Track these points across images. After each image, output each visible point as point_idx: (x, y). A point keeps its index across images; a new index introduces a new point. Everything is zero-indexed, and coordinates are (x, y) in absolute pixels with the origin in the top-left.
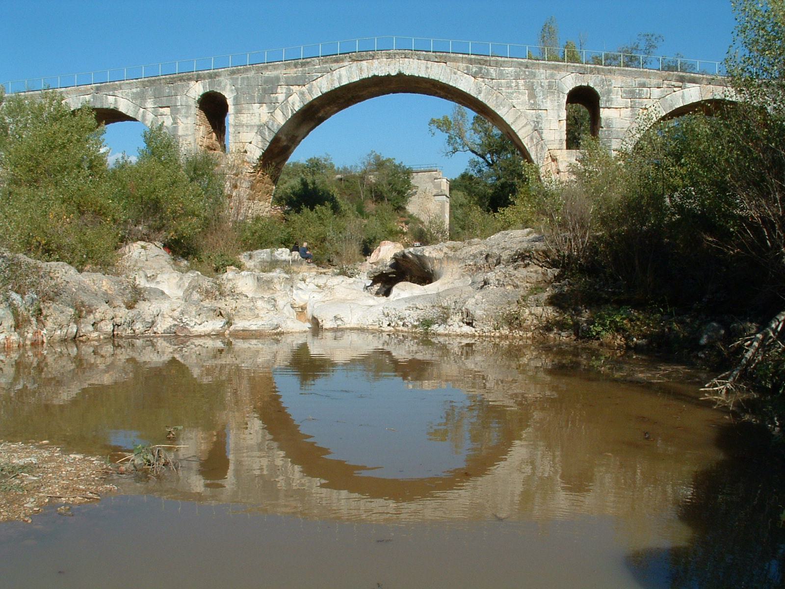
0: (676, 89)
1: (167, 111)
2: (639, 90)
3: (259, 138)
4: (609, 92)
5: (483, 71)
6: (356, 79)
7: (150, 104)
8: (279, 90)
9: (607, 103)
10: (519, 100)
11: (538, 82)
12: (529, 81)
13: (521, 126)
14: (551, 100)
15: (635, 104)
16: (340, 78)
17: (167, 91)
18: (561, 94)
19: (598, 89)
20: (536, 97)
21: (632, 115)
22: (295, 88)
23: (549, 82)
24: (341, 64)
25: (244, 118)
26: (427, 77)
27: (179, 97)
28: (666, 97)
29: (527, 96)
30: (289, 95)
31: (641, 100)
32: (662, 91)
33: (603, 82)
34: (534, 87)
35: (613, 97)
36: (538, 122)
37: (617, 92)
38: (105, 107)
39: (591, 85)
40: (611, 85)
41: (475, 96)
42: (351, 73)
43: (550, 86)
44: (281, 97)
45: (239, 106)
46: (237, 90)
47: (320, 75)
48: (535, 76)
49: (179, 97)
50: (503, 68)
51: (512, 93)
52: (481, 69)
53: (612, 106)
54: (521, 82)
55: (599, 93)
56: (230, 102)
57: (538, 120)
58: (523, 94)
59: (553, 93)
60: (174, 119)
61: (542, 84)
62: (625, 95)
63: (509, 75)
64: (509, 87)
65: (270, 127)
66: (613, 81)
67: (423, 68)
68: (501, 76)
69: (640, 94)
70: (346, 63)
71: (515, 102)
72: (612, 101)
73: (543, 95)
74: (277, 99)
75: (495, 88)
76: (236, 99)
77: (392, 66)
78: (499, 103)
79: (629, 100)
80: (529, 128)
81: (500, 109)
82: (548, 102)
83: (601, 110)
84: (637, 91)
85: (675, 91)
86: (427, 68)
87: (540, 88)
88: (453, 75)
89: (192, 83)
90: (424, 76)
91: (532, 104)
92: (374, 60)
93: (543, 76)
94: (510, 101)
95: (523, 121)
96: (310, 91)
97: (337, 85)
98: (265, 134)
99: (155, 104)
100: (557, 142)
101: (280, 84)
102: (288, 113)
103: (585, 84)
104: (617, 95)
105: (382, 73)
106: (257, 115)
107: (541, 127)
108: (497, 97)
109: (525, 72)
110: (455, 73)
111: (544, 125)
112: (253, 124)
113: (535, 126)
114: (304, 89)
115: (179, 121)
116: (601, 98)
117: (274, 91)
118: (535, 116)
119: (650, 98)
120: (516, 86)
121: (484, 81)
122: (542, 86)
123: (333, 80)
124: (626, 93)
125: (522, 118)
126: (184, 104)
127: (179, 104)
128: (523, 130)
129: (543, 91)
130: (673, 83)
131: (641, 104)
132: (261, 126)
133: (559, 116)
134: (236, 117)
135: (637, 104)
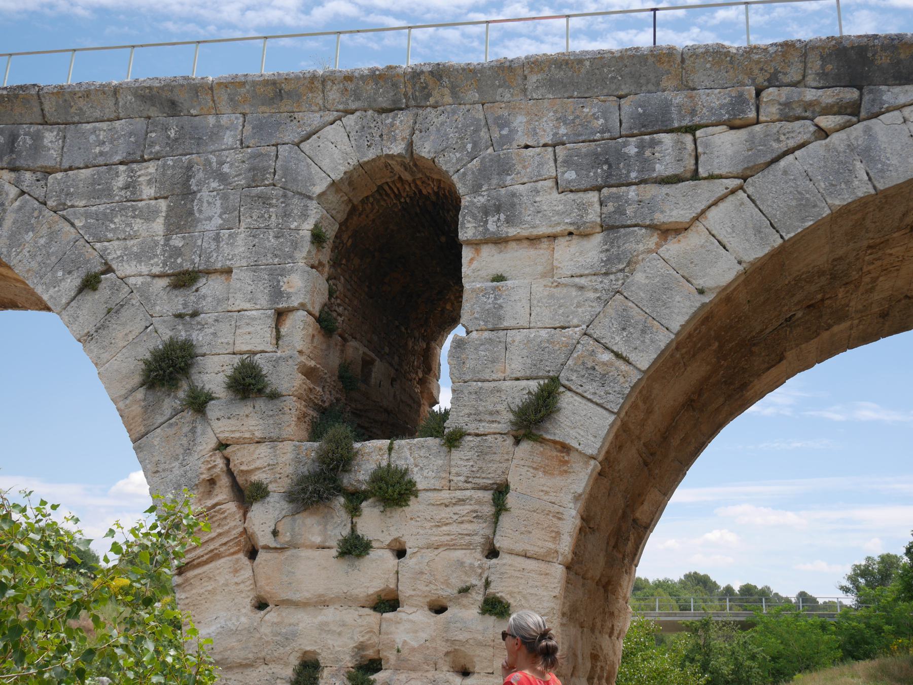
0: (826, 122)
2: (641, 147)
9: (491, 220)
10: (130, 243)
11: (208, 162)
14: (253, 232)
15: (620, 211)
21: (609, 261)
23: (254, 156)
28: (783, 163)
29: (160, 220)
32: (751, 140)
33: (476, 131)
34: (193, 181)
39: (425, 150)
40: (506, 140)
50: (89, 126)
51: (107, 218)
58: (149, 216)
59: (265, 200)
62: (571, 175)
66: (519, 121)
72: (513, 205)
73: (225, 210)
75: (51, 203)
79: (593, 197)
82: (241, 239)
83: (467, 254)
84: (632, 150)
85: (823, 133)
87: (214, 185)
94: (98, 246)
108: (53, 236)
116: (464, 202)
120: (127, 187)
121: (16, 183)
124: (578, 168)
125: (125, 313)
129: (225, 197)
130: (810, 95)
133: (277, 293)
135: (629, 211)
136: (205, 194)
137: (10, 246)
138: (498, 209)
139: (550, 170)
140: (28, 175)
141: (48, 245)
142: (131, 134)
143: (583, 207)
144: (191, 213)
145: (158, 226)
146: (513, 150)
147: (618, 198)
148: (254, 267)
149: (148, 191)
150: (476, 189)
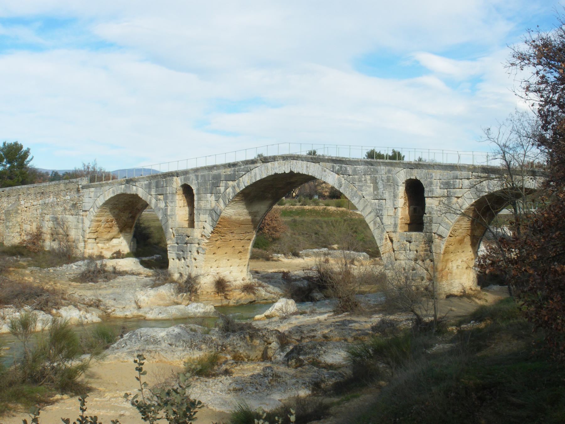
1: (161, 197)
2: (453, 181)
3: (210, 218)
4: (431, 183)
5: (343, 169)
6: (264, 176)
7: (153, 192)
8: (221, 184)
11: (379, 177)
12: (374, 176)
13: (367, 213)
14: (389, 192)
16: (255, 175)
17: (162, 183)
18: (396, 186)
19: (422, 181)
20: (378, 189)
22: (230, 183)
23: (387, 176)
24: (256, 165)
25: (203, 204)
26: (307, 174)
27: (168, 188)
30: (226, 189)
31: (455, 190)
35: (434, 188)
36: (380, 210)
37: (437, 183)
38: (132, 193)
39: (418, 178)
40: (431, 178)
41: (338, 189)
42: (262, 172)
43: (388, 179)
44: (222, 189)
45: (199, 195)
46: (198, 183)
47: (244, 173)
48: (377, 172)
49: (168, 188)
51: (362, 186)
52: (341, 167)
53: (434, 196)
54: (368, 177)
55: (423, 184)
56: (195, 192)
57: (380, 208)
58: (369, 187)
59: (390, 185)
60: (166, 203)
61: (383, 178)
62: (442, 186)
63: (360, 172)
64: (360, 181)
65: (216, 211)
66: (434, 174)
67: (305, 168)
68: (355, 172)
69: (454, 185)
70: (258, 165)
71: (364, 193)
74: (220, 190)
76: (198, 190)
77: (286, 166)
78: (353, 195)
80: (373, 214)
81: (354, 200)
82: (387, 193)
83: (426, 199)
86: (307, 167)
88: (323, 173)
89: (175, 178)
90: (305, 173)
91: (376, 195)
92: (275, 162)
93: (383, 172)
95: (369, 209)
96: (238, 185)
97: (254, 181)
98: (213, 216)
99: (156, 192)
100: (392, 226)
101: (222, 180)
102: (226, 201)
103: (413, 177)
104: (437, 186)
105: (280, 171)
106: (210, 202)
107: (381, 214)
108: (352, 190)
109: (371, 169)
110: (325, 171)
111: (385, 213)
112: (207, 208)
113: (377, 213)
114: (235, 183)
115: (168, 205)
116: (425, 189)
117: (216, 185)
118: (377, 205)
119: (462, 188)
120: (365, 180)
121: (343, 177)
122: (382, 180)
123: (251, 177)
125: (368, 207)
126: (171, 193)
127: (168, 193)
128: (369, 216)
129: (383, 184)
131: (455, 193)
132: (211, 210)
134: (198, 203)
135: (451, 194)
136: (379, 183)
137: (344, 191)
138: (430, 192)
139: (439, 184)
140: (345, 176)
141: (352, 191)
142: (364, 169)
143: (444, 192)
144: (377, 187)
145: (372, 189)
146: (433, 180)
147: (449, 191)
148: (390, 199)
149: (369, 182)
150: (427, 187)
